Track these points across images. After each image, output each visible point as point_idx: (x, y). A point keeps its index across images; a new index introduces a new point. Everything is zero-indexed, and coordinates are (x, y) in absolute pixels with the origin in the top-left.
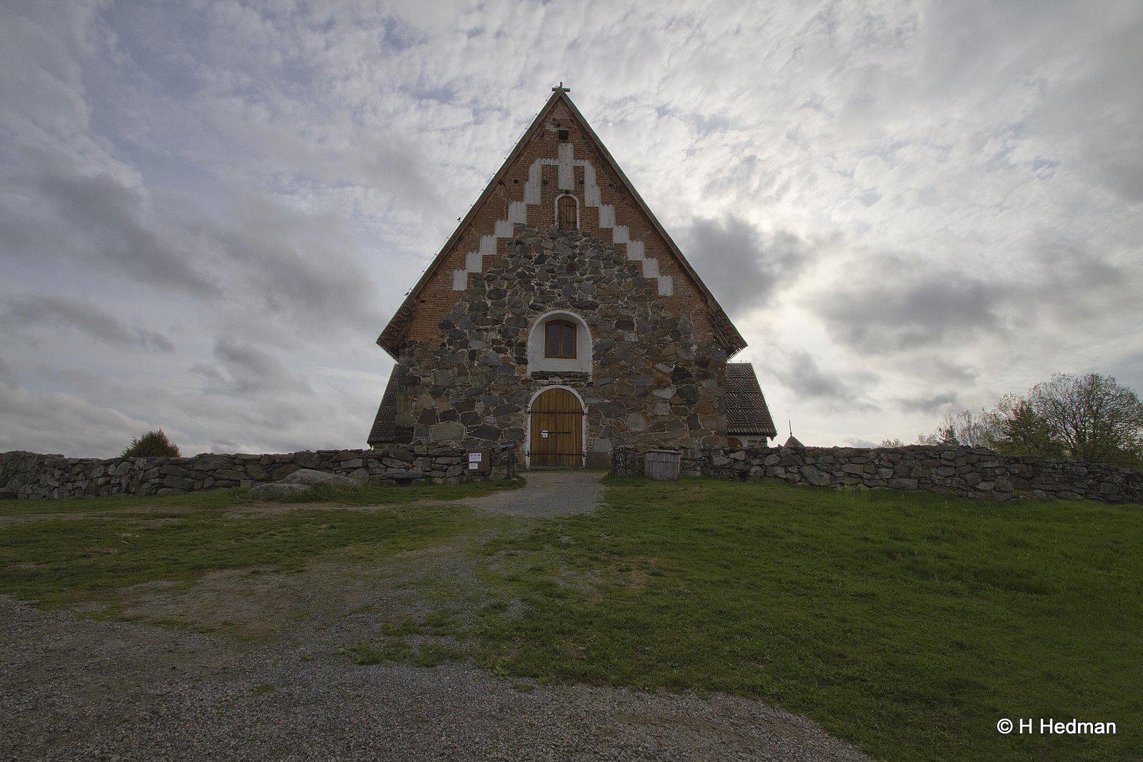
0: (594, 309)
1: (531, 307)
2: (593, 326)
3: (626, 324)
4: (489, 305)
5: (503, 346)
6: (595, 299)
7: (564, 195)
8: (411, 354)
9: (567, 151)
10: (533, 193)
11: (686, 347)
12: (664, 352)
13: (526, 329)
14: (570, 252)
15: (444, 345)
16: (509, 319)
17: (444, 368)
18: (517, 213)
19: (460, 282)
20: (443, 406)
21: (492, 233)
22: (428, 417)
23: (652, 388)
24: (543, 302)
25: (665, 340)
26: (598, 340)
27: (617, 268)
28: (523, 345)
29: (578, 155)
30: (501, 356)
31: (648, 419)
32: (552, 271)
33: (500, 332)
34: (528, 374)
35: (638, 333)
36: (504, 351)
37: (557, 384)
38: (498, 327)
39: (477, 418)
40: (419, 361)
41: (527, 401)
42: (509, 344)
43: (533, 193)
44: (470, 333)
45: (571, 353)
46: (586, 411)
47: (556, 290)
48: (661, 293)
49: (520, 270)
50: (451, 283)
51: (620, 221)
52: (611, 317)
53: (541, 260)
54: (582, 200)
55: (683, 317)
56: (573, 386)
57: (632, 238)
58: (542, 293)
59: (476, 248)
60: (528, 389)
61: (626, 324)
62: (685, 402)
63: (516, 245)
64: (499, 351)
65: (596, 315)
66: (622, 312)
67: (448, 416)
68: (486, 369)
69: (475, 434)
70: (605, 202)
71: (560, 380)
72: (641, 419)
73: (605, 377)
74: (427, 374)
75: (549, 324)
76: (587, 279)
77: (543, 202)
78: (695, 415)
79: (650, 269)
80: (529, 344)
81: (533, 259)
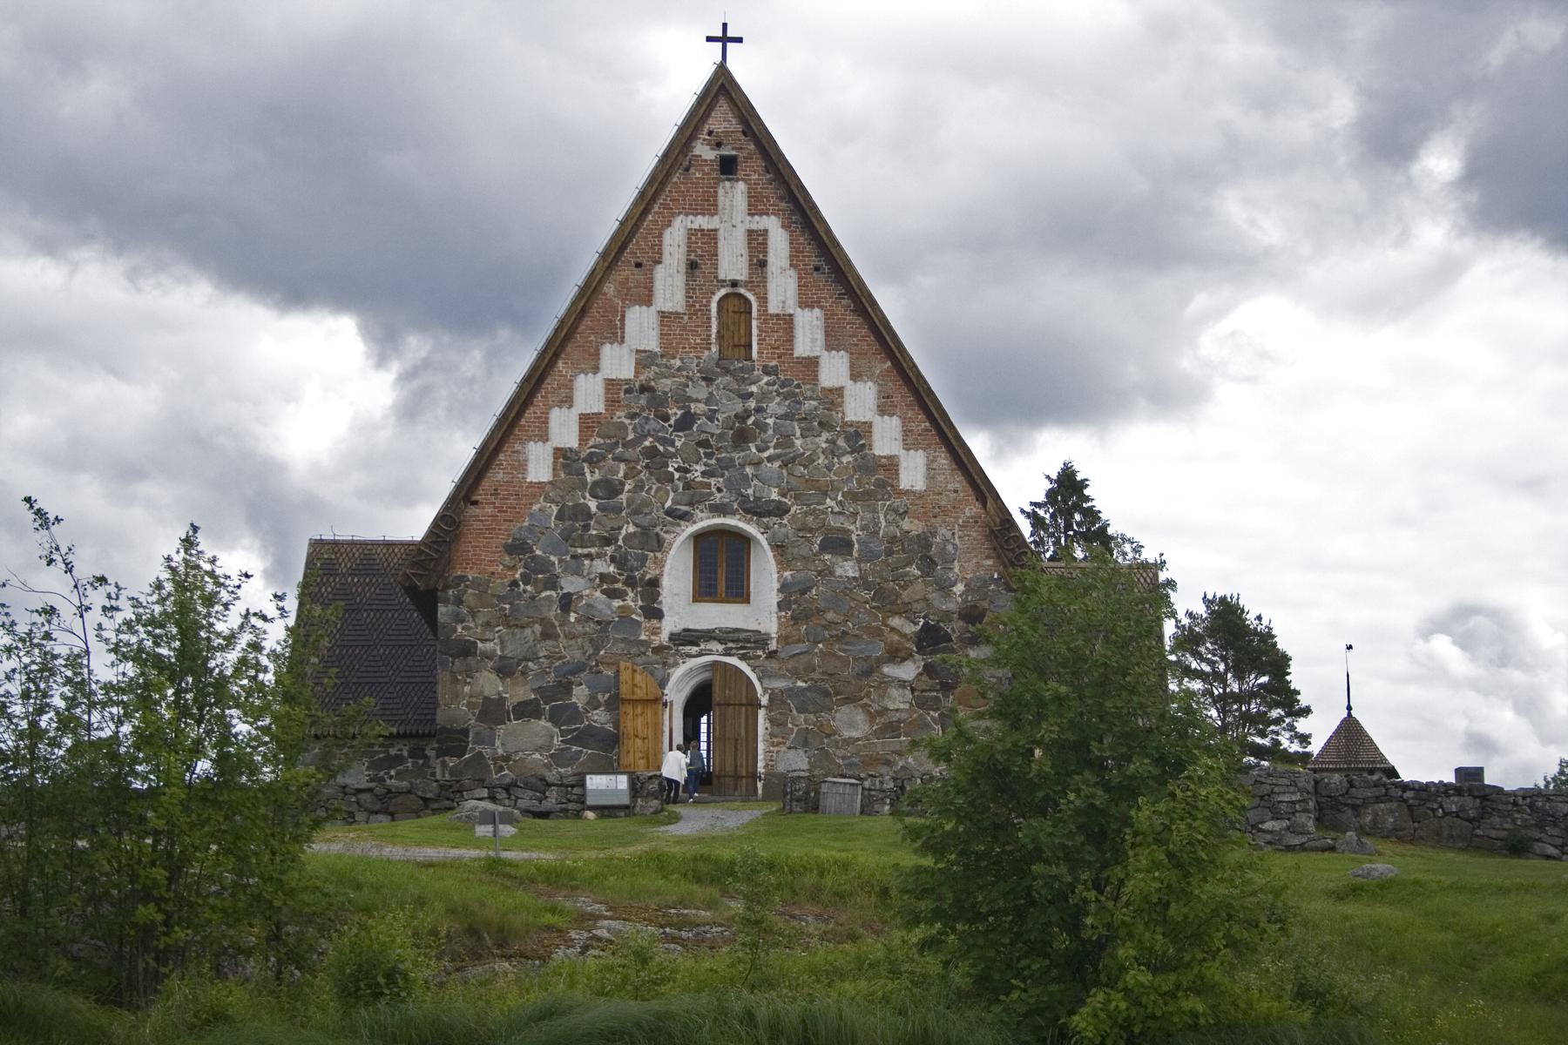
0: (781, 516)
1: (669, 513)
2: (779, 547)
3: (838, 544)
4: (594, 509)
5: (619, 586)
6: (784, 495)
8: (459, 601)
9: (734, 196)
10: (670, 286)
11: (945, 588)
13: (659, 555)
14: (739, 408)
15: (514, 584)
18: (642, 328)
19: (539, 466)
20: (520, 693)
22: (493, 712)
23: (881, 661)
24: (690, 504)
25: (907, 574)
26: (787, 574)
27: (825, 435)
28: (654, 583)
30: (617, 603)
31: (872, 717)
32: (704, 444)
33: (613, 559)
34: (664, 637)
35: (859, 561)
36: (619, 595)
37: (715, 653)
38: (609, 550)
42: (631, 582)
43: (670, 286)
44: (560, 561)
46: (764, 701)
47: (713, 481)
49: (647, 443)
50: (522, 466)
51: (833, 341)
52: (811, 530)
53: (686, 422)
54: (763, 300)
55: (942, 531)
56: (743, 658)
57: (855, 376)
58: (688, 485)
59: (568, 401)
60: (665, 664)
61: (838, 544)
63: (638, 393)
64: (612, 594)
65: (784, 526)
66: (835, 522)
67: (526, 710)
68: (590, 627)
69: (577, 740)
70: (805, 303)
71: (720, 648)
72: (860, 717)
73: (799, 641)
74: (488, 635)
75: (702, 540)
76: (770, 459)
77: (689, 306)
79: (887, 438)
80: (666, 582)
81: (672, 422)
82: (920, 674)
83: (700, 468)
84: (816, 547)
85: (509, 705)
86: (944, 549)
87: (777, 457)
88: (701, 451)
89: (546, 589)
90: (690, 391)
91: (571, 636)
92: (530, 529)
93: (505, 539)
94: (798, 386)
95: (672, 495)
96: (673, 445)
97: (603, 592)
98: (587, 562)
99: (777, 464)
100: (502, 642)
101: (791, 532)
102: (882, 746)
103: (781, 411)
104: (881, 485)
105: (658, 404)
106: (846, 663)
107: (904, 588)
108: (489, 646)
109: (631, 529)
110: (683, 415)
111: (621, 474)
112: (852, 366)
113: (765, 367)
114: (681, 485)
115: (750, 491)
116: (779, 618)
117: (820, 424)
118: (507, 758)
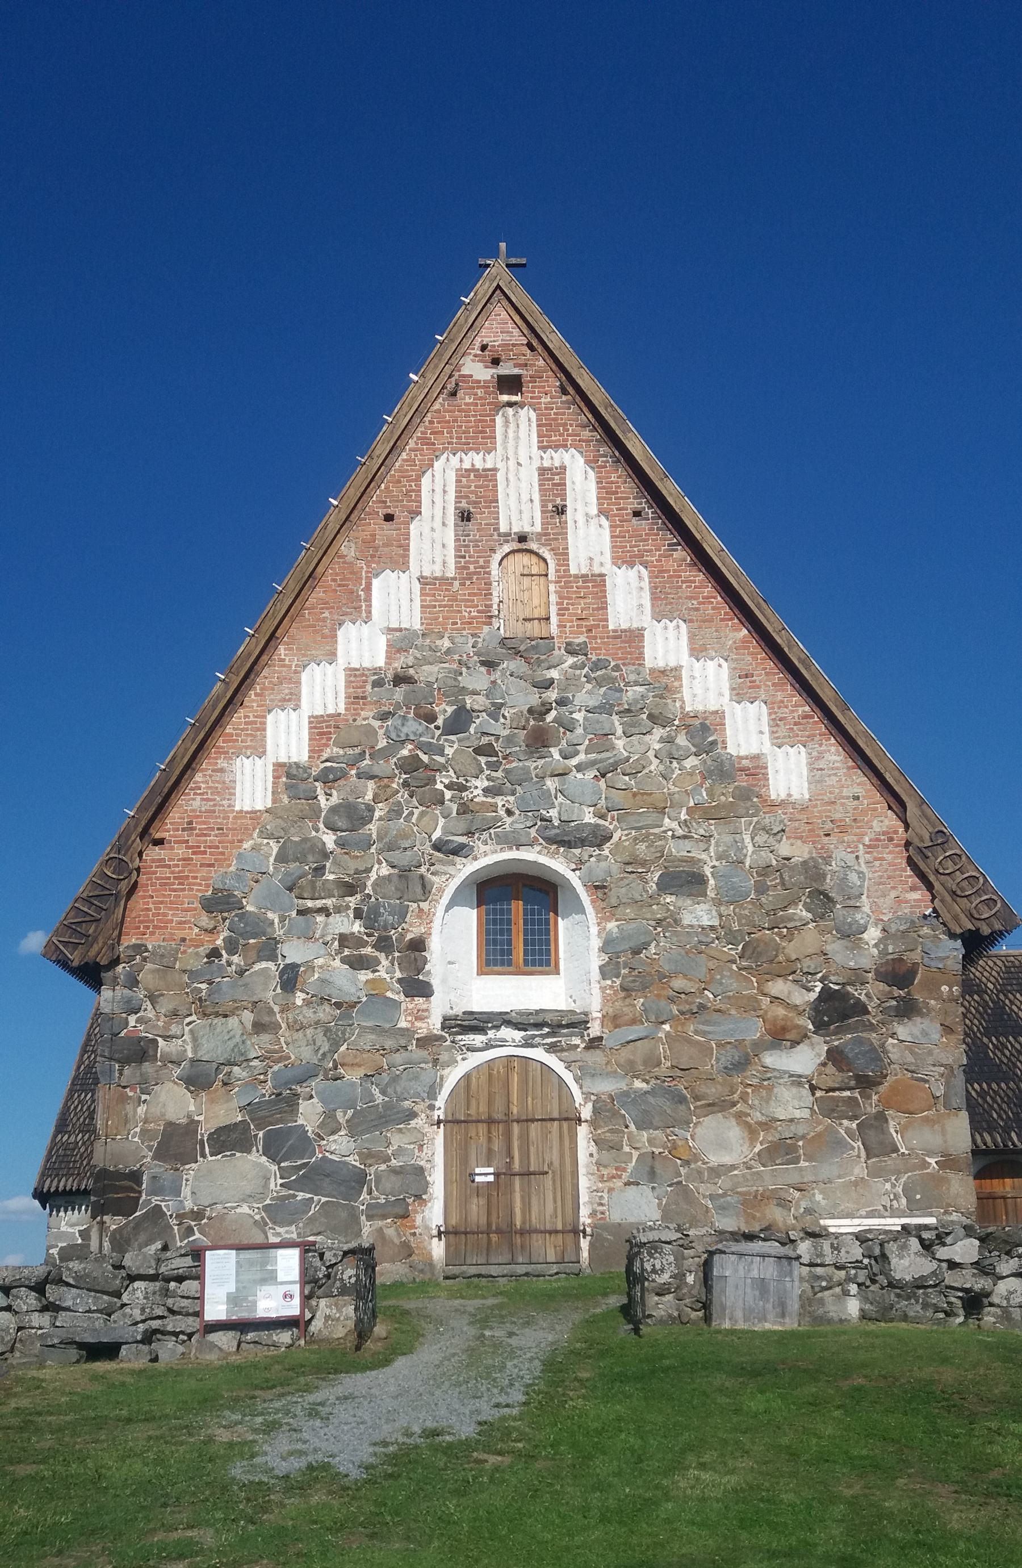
0: (599, 846)
1: (437, 847)
2: (599, 888)
3: (687, 881)
5: (368, 950)
6: (602, 817)
7: (515, 546)
8: (133, 982)
11: (851, 935)
12: (792, 950)
13: (424, 906)
14: (534, 699)
16: (381, 881)
17: (217, 1015)
20: (216, 1113)
21: (332, 657)
22: (178, 1144)
23: (759, 1047)
24: (469, 833)
25: (791, 919)
26: (612, 925)
27: (659, 732)
28: (418, 945)
29: (549, 437)
30: (364, 976)
31: (752, 1132)
33: (358, 914)
34: (434, 1024)
35: (718, 903)
38: (352, 901)
39: (303, 1144)
40: (153, 998)
41: (432, 1093)
42: (384, 945)
44: (282, 919)
46: (586, 1113)
47: (500, 801)
50: (228, 790)
51: (664, 605)
53: (458, 723)
54: (563, 556)
55: (840, 855)
56: (552, 1048)
57: (698, 651)
59: (292, 700)
60: (436, 1062)
61: (687, 881)
62: (853, 1083)
64: (358, 963)
65: (604, 861)
66: (677, 849)
67: (229, 1140)
68: (325, 1013)
69: (301, 1184)
70: (624, 558)
71: (518, 1035)
72: (734, 1132)
73: (634, 1022)
74: (174, 1029)
76: (579, 768)
78: (881, 1118)
80: (435, 944)
81: (440, 722)
82: (824, 1064)
83: (482, 783)
85: (204, 1132)
86: (845, 878)
87: (592, 764)
88: (483, 760)
89: (260, 959)
90: (466, 681)
91: (296, 1027)
92: (238, 876)
94: (617, 668)
95: (441, 822)
97: (343, 961)
98: (320, 919)
99: (591, 774)
100: (195, 1039)
101: (615, 868)
102: (774, 1177)
103: (592, 703)
104: (744, 795)
106: (705, 1050)
107: (789, 937)
109: (385, 870)
110: (455, 711)
111: (369, 796)
112: (692, 637)
114: (455, 807)
115: (553, 813)
116: (603, 989)
117: (651, 717)
118: (198, 1215)
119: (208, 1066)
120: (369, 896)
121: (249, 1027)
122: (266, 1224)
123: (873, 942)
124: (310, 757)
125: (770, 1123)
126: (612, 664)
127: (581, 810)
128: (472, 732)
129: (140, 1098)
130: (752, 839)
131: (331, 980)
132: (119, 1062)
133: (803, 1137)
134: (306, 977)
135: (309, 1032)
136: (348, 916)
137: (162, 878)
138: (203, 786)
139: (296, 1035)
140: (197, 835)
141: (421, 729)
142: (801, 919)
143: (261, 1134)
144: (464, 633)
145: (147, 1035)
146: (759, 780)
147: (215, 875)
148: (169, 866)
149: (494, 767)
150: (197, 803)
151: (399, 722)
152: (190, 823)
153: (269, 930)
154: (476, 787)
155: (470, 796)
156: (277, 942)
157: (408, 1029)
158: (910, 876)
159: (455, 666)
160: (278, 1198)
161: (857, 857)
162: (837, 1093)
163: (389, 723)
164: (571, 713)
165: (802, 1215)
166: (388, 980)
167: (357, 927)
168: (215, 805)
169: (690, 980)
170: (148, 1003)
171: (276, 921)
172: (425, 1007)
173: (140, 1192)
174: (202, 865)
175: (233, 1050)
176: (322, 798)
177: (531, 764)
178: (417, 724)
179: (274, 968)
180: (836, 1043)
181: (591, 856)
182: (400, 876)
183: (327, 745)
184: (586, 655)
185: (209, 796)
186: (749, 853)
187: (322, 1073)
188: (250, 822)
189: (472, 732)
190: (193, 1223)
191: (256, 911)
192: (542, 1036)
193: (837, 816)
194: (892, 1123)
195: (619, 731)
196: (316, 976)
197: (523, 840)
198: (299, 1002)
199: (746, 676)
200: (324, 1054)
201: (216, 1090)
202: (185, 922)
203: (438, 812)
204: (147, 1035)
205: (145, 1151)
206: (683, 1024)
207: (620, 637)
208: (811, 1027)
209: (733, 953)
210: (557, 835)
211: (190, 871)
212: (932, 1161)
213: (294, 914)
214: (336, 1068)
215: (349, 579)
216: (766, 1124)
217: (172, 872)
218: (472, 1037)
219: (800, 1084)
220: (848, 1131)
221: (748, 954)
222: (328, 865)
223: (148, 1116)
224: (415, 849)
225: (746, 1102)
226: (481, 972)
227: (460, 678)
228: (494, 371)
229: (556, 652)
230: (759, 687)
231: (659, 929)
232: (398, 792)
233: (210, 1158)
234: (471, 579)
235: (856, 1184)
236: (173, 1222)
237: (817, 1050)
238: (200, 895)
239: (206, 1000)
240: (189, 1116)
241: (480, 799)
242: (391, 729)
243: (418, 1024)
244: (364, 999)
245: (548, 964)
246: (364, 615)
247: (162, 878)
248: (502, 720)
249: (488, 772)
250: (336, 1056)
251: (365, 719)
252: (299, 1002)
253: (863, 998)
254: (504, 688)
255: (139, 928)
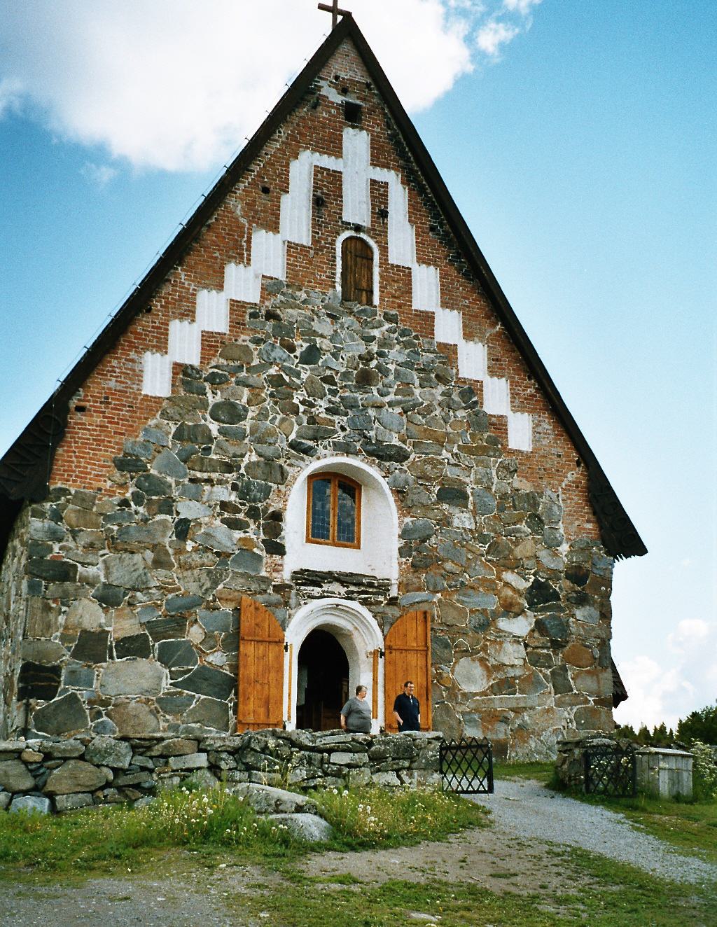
1: (293, 445)
3: (454, 494)
4: (215, 433)
5: (241, 516)
6: (404, 442)
7: (352, 233)
8: (57, 516)
9: (357, 142)
11: (552, 545)
14: (362, 349)
17: (126, 551)
19: (156, 378)
20: (122, 625)
21: (220, 287)
22: (92, 647)
24: (315, 439)
25: (519, 531)
26: (408, 520)
27: (441, 388)
28: (277, 517)
30: (238, 534)
31: (489, 670)
32: (329, 380)
33: (235, 487)
34: (286, 576)
35: (474, 514)
38: (231, 477)
39: (189, 653)
40: (74, 534)
42: (253, 513)
44: (178, 483)
45: (348, 536)
47: (336, 418)
48: (513, 444)
50: (137, 377)
52: (429, 479)
53: (311, 355)
54: (384, 249)
56: (365, 602)
57: (468, 336)
58: (312, 420)
59: (189, 314)
61: (454, 494)
64: (233, 525)
65: (405, 473)
66: (450, 472)
67: (133, 647)
68: (209, 558)
69: (188, 684)
71: (343, 590)
72: (478, 671)
73: (419, 589)
74: (90, 559)
75: (319, 481)
76: (390, 404)
77: (315, 241)
79: (497, 397)
81: (298, 353)
82: (533, 631)
83: (323, 404)
84: (434, 497)
85: (111, 640)
86: (550, 509)
87: (398, 403)
88: (327, 387)
89: (161, 512)
90: (316, 325)
92: (145, 445)
93: (112, 453)
94: (416, 337)
95: (296, 427)
96: (298, 375)
97: (222, 521)
98: (207, 487)
99: (398, 410)
100: (107, 568)
101: (411, 479)
102: (500, 702)
103: (402, 359)
105: (284, 334)
106: (462, 613)
107: (516, 543)
108: (91, 571)
109: (254, 458)
110: (309, 348)
111: (244, 400)
113: (386, 314)
114: (305, 418)
115: (372, 433)
116: (400, 564)
117: (437, 376)
119: (117, 589)
120: (243, 475)
121: (150, 562)
122: (158, 712)
123: (564, 553)
124: (201, 362)
125: (501, 667)
126: (414, 334)
127: (390, 434)
128: (320, 364)
129: (61, 609)
130: (497, 474)
131: (214, 534)
132: (45, 579)
133: (519, 678)
134: (195, 530)
135: (196, 572)
136: (227, 488)
137: (84, 439)
138: (117, 370)
139: (185, 574)
140: (112, 409)
141: (285, 356)
142: (524, 532)
143: (157, 645)
144: (317, 290)
145: (68, 560)
146: (502, 433)
147: (128, 442)
148: (89, 430)
149: (334, 393)
150: (112, 384)
151: (270, 348)
152: (107, 398)
153: (168, 491)
154: (321, 406)
155: (317, 412)
156: (174, 501)
157: (267, 578)
158: (587, 513)
159: (309, 313)
160: (168, 694)
161: (558, 496)
162: (539, 651)
163: (262, 347)
164: (387, 364)
165: (516, 729)
166: (255, 540)
167: (233, 498)
168: (126, 387)
169: (456, 564)
170: (70, 535)
171: (173, 485)
172: (280, 562)
173: (59, 682)
174: (115, 433)
175: (137, 579)
176: (210, 395)
177: (359, 396)
178: (281, 351)
179: (171, 520)
180: (540, 617)
181: (396, 469)
182: (265, 464)
183: (214, 356)
184: (397, 323)
185: (122, 379)
186: (495, 483)
187: (205, 603)
188: (154, 405)
189: (320, 364)
190: (102, 709)
191: (159, 475)
192: (358, 592)
193: (548, 466)
194: (569, 673)
195: (417, 382)
196: (203, 530)
197: (352, 450)
198: (189, 548)
199: (497, 360)
200: (207, 590)
201: (123, 609)
202: (101, 476)
203: (293, 420)
204: (68, 560)
205: (65, 651)
206: (450, 595)
207: (420, 316)
208: (526, 605)
209: (482, 549)
210: (374, 450)
211: (106, 436)
212: (591, 699)
213: (186, 481)
214: (214, 601)
215: (235, 231)
216: (497, 667)
217: (91, 435)
218: (312, 588)
219: (519, 642)
220: (545, 676)
221: (491, 551)
222: (213, 447)
223: (69, 623)
224: (277, 445)
225: (486, 651)
226: (308, 541)
227: (312, 323)
228: (344, 98)
229: (377, 318)
230: (504, 369)
231: (438, 527)
232: (265, 400)
233: (117, 660)
234: (322, 251)
235: (548, 711)
236: (86, 706)
237: (529, 619)
238: (113, 456)
239: (117, 539)
240: (100, 626)
241: (323, 415)
242: (264, 352)
243: (275, 575)
244: (237, 552)
245: (353, 541)
246: (245, 261)
247: (84, 439)
248: (341, 360)
249: (330, 397)
250: (214, 592)
251: (243, 341)
252: (189, 548)
253: (557, 589)
254: (342, 336)
255: (63, 475)
